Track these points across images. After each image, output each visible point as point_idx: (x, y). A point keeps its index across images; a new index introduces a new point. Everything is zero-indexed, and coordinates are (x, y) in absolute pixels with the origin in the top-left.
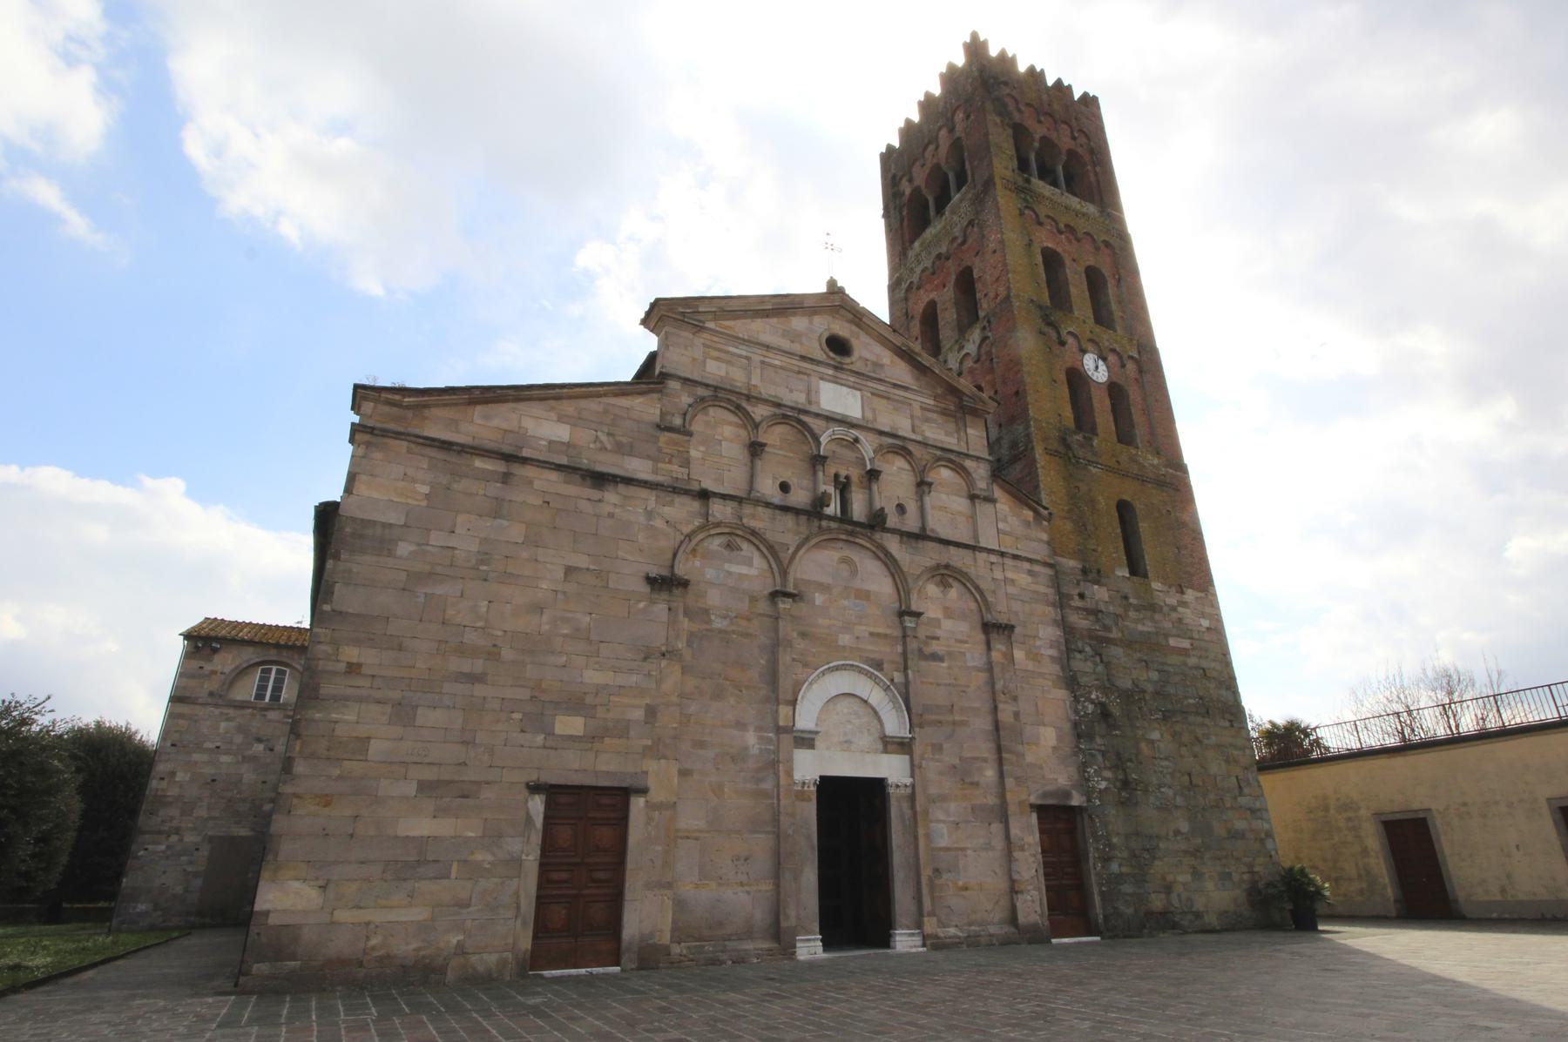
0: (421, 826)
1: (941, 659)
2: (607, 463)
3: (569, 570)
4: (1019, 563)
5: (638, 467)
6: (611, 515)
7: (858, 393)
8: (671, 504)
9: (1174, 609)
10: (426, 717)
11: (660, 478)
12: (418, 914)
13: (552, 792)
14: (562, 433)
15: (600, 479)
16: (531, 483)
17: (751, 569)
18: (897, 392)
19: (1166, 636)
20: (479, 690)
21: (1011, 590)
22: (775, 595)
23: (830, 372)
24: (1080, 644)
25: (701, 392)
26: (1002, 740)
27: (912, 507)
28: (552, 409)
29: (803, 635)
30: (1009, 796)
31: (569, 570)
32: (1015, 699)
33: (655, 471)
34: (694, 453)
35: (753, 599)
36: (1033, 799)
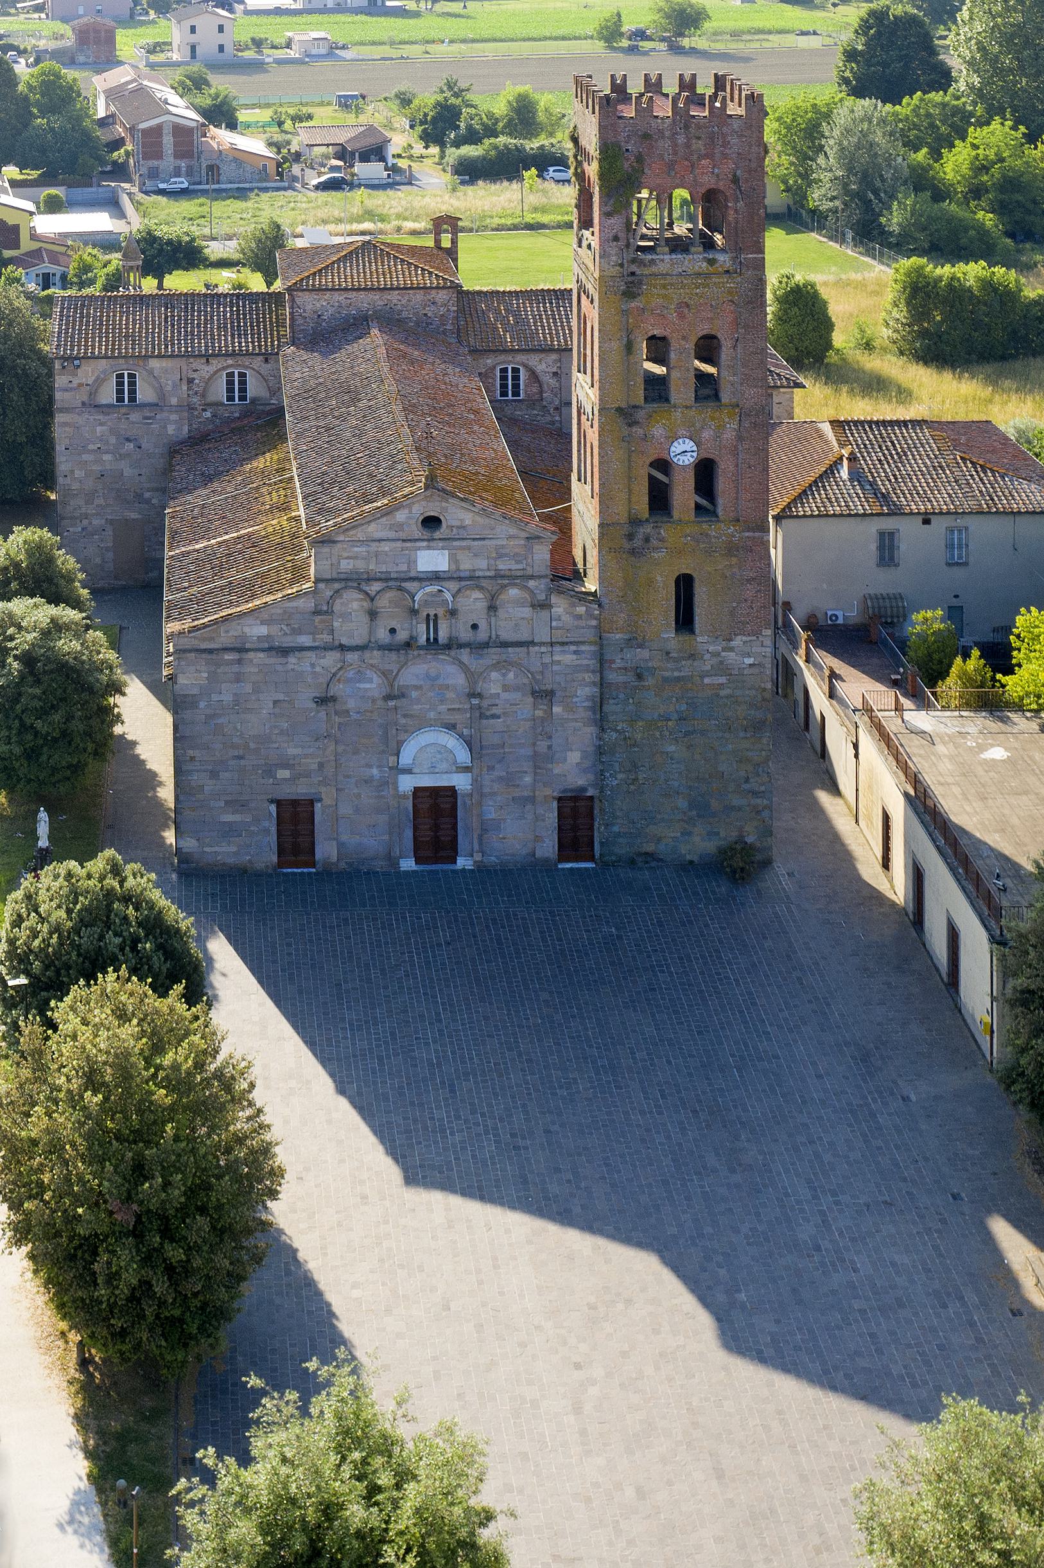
0: (229, 818)
1: (499, 717)
2: (288, 641)
3: (275, 702)
4: (566, 648)
5: (305, 640)
6: (293, 670)
7: (446, 552)
8: (324, 657)
9: (718, 654)
10: (224, 775)
11: (317, 644)
12: (234, 849)
13: (279, 803)
14: (263, 630)
15: (285, 652)
16: (251, 661)
17: (374, 685)
18: (476, 543)
19: (702, 677)
20: (242, 762)
21: (555, 668)
22: (388, 697)
23: (425, 544)
24: (614, 693)
25: (337, 586)
26: (540, 762)
27: (483, 625)
28: (257, 618)
29: (405, 716)
30: (537, 793)
31: (275, 702)
32: (550, 737)
33: (314, 640)
34: (335, 624)
35: (374, 701)
36: (555, 794)
